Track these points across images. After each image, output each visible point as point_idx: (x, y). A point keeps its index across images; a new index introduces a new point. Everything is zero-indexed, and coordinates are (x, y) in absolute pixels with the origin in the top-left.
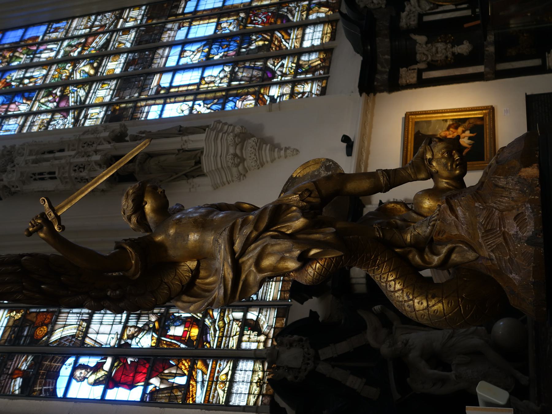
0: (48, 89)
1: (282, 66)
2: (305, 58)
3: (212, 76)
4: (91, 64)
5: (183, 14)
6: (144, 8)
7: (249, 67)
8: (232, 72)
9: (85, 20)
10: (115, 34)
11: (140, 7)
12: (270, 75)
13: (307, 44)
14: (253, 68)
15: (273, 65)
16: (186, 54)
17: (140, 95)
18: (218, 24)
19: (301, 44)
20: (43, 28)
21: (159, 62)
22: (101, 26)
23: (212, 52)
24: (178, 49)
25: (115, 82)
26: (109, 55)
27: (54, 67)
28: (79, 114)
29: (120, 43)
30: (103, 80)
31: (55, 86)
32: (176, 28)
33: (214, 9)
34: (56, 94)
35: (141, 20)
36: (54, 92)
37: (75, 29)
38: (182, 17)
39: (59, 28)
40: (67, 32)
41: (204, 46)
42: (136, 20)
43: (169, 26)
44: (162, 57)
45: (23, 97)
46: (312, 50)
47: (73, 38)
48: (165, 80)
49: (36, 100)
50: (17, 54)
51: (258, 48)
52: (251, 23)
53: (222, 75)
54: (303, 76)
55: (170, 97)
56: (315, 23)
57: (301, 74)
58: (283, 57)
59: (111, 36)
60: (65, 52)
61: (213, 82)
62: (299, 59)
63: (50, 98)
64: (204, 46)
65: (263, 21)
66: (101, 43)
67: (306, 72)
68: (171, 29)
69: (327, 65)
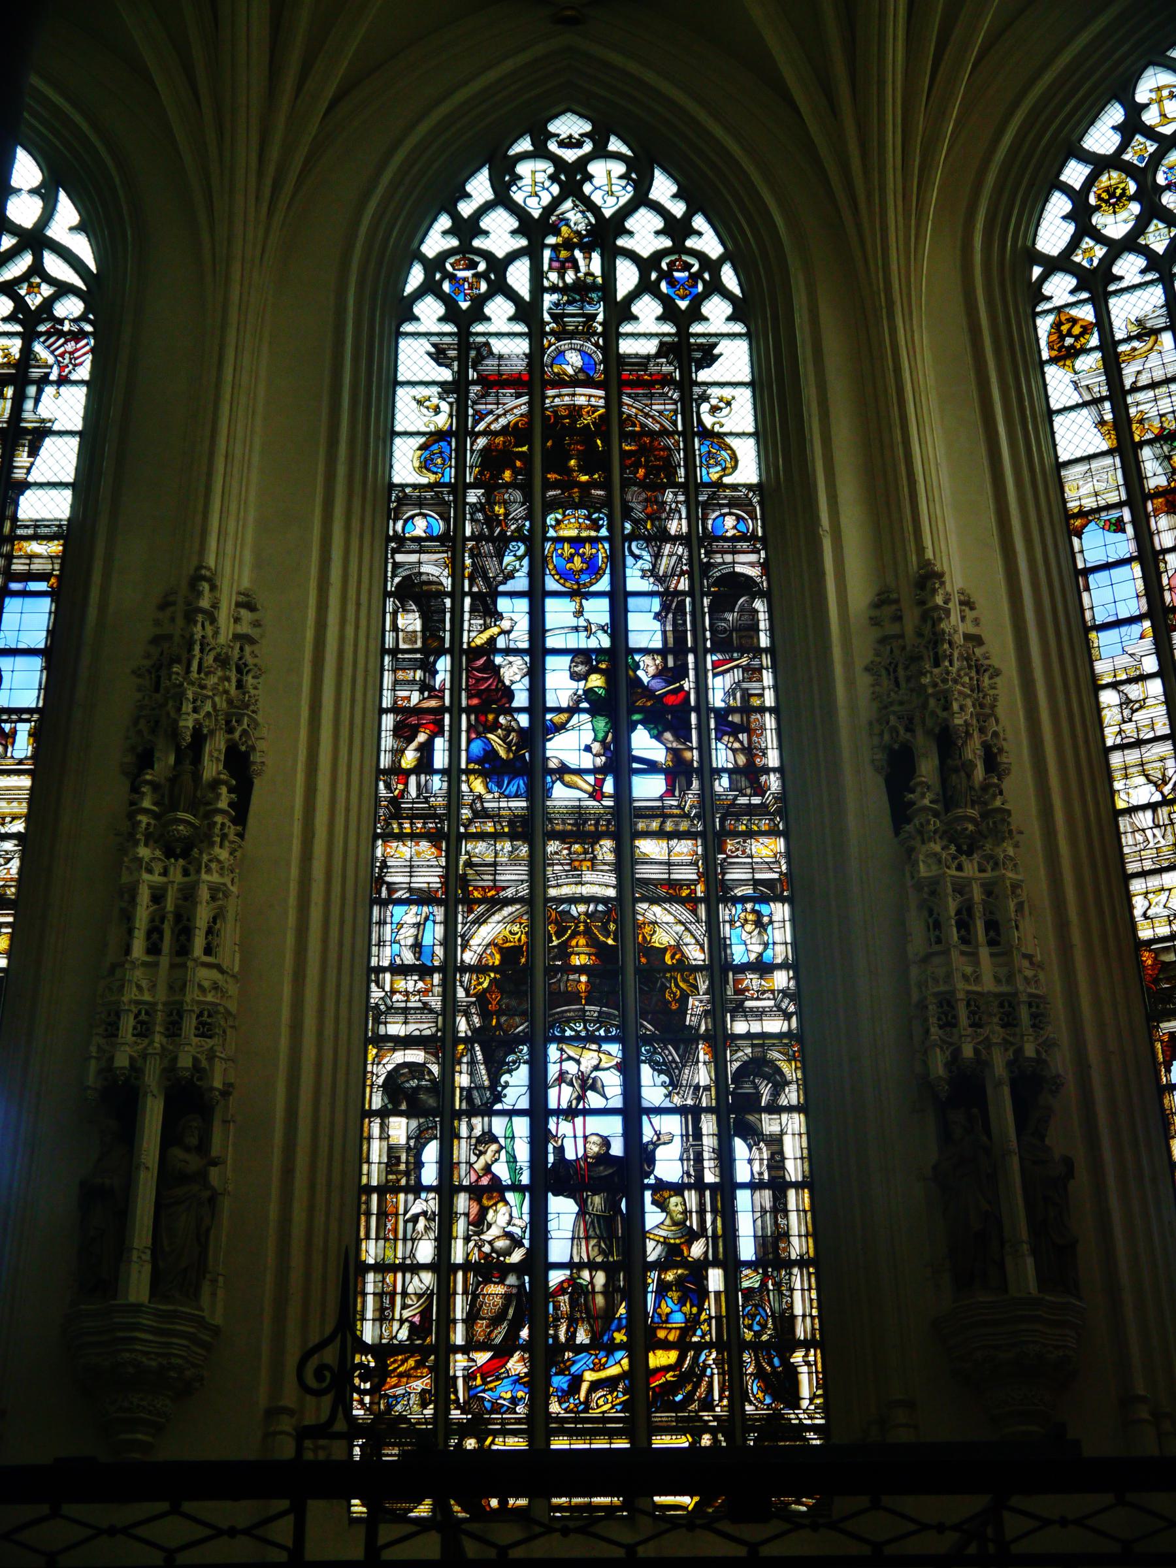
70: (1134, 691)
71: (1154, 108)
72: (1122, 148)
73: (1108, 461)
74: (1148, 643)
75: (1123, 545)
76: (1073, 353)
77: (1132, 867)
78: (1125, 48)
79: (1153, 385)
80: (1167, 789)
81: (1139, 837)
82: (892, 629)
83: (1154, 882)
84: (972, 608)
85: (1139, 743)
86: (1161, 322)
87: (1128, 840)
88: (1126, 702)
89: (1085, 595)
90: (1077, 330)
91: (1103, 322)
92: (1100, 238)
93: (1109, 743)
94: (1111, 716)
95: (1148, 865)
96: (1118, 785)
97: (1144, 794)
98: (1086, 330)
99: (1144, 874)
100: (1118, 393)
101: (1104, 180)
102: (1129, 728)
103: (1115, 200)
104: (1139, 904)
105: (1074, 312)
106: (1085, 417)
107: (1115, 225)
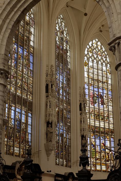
0: (16, 72)
1: (11, 142)
2: (12, 148)
3: (12, 122)
4: (20, 85)
5: (28, 112)
6: (32, 100)
7: (12, 132)
8: (12, 127)
9: (31, 82)
10: (26, 92)
11: (32, 99)
12: (10, 138)
13: (15, 148)
14: (12, 134)
15: (12, 139)
16: (18, 114)
17: (11, 101)
18: (24, 123)
19: (16, 147)
20: (32, 69)
21: (17, 106)
22: (29, 87)
23: (18, 122)
24: (20, 112)
25: (15, 93)
26: (22, 90)
27: (21, 73)
28: (9, 82)
29: (24, 94)
30: (16, 89)
31: (17, 74)
32: (25, 111)
33: (28, 121)
34: (15, 75)
35: (29, 100)
36: (15, 74)
37: (30, 79)
38: (27, 112)
39: (31, 74)
40: (29, 77)
41: (20, 119)
42: (29, 98)
43: (26, 109)
44: (19, 107)
45: (16, 64)
46: (13, 149)
47: (28, 79)
48: (13, 108)
49: (14, 68)
50: (27, 61)
51: (16, 135)
52: (23, 133)
53: (12, 124)
54: (8, 147)
55: (9, 110)
56: (20, 151)
57: (9, 147)
58: (13, 142)
59: (26, 91)
60: (25, 76)
61: (11, 122)
62: (12, 146)
63: (14, 73)
64: (20, 119)
65: (22, 136)
66: (25, 88)
67: (9, 148)
68: (25, 109)
69: (10, 154)
82: (81, 91)
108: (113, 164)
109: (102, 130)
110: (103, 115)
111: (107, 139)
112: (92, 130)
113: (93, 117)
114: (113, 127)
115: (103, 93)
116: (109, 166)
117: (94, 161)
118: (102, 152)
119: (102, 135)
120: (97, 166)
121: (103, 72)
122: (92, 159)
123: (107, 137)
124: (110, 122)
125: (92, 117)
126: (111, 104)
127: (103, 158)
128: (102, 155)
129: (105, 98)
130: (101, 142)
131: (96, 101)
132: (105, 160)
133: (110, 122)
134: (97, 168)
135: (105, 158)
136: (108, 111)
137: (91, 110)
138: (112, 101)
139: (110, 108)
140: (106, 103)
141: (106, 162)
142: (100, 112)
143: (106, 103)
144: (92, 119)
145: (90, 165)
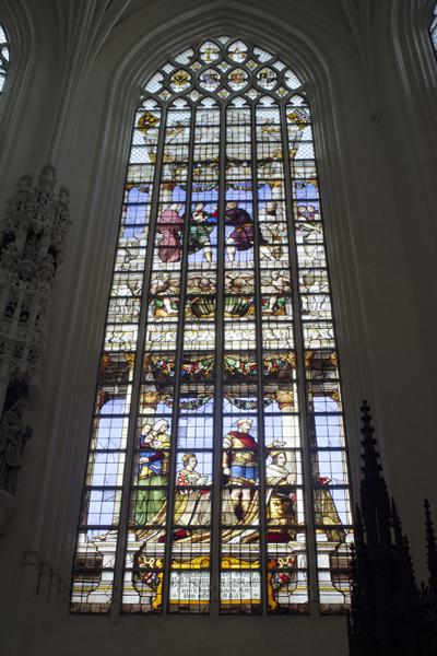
70: (133, 252)
71: (206, 55)
72: (189, 65)
73: (149, 167)
74: (145, 235)
75: (146, 198)
76: (148, 127)
77: (110, 320)
78: (201, 28)
79: (177, 144)
80: (135, 292)
81: (117, 309)
83: (118, 328)
84: (68, 195)
85: (129, 272)
86: (187, 124)
87: (112, 309)
88: (129, 255)
89: (124, 214)
90: (152, 120)
91: (164, 120)
92: (171, 91)
93: (116, 270)
94: (120, 260)
95: (118, 321)
96: (115, 287)
97: (124, 291)
98: (155, 121)
99: (114, 324)
100: (162, 144)
101: (179, 73)
102: (126, 265)
103: (181, 80)
104: (109, 336)
105: (153, 114)
106: (145, 151)
107: (178, 88)
108: (331, 554)
109: (232, 362)
110: (247, 290)
111: (276, 405)
112: (156, 373)
113: (170, 311)
114: (336, 339)
115: (255, 202)
116: (294, 570)
117: (155, 546)
118: (231, 488)
119: (236, 388)
120: (174, 575)
121: (258, 129)
122: (131, 537)
123: (282, 392)
124: (304, 317)
125: (161, 312)
126: (317, 235)
127: (231, 520)
128: (227, 507)
129: (272, 218)
130: (226, 431)
131: (203, 239)
132: (249, 532)
133: (304, 317)
134: (174, 590)
135: (256, 522)
136: (294, 267)
137: (153, 282)
138: (322, 221)
139: (311, 255)
140: (274, 238)
141: (264, 548)
142: (227, 281)
143: (274, 238)
144: (163, 323)
145: (108, 577)
